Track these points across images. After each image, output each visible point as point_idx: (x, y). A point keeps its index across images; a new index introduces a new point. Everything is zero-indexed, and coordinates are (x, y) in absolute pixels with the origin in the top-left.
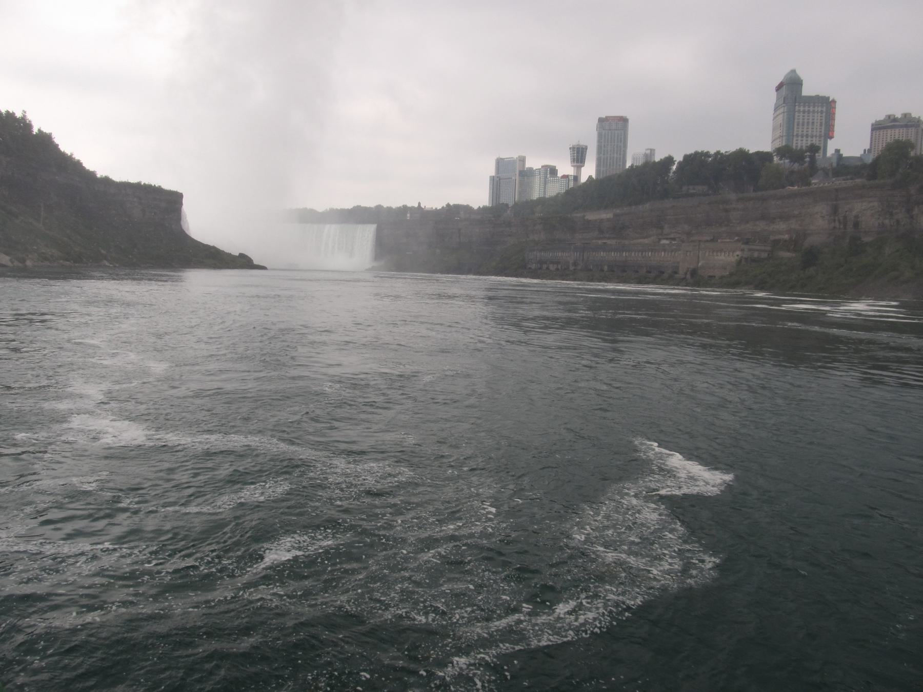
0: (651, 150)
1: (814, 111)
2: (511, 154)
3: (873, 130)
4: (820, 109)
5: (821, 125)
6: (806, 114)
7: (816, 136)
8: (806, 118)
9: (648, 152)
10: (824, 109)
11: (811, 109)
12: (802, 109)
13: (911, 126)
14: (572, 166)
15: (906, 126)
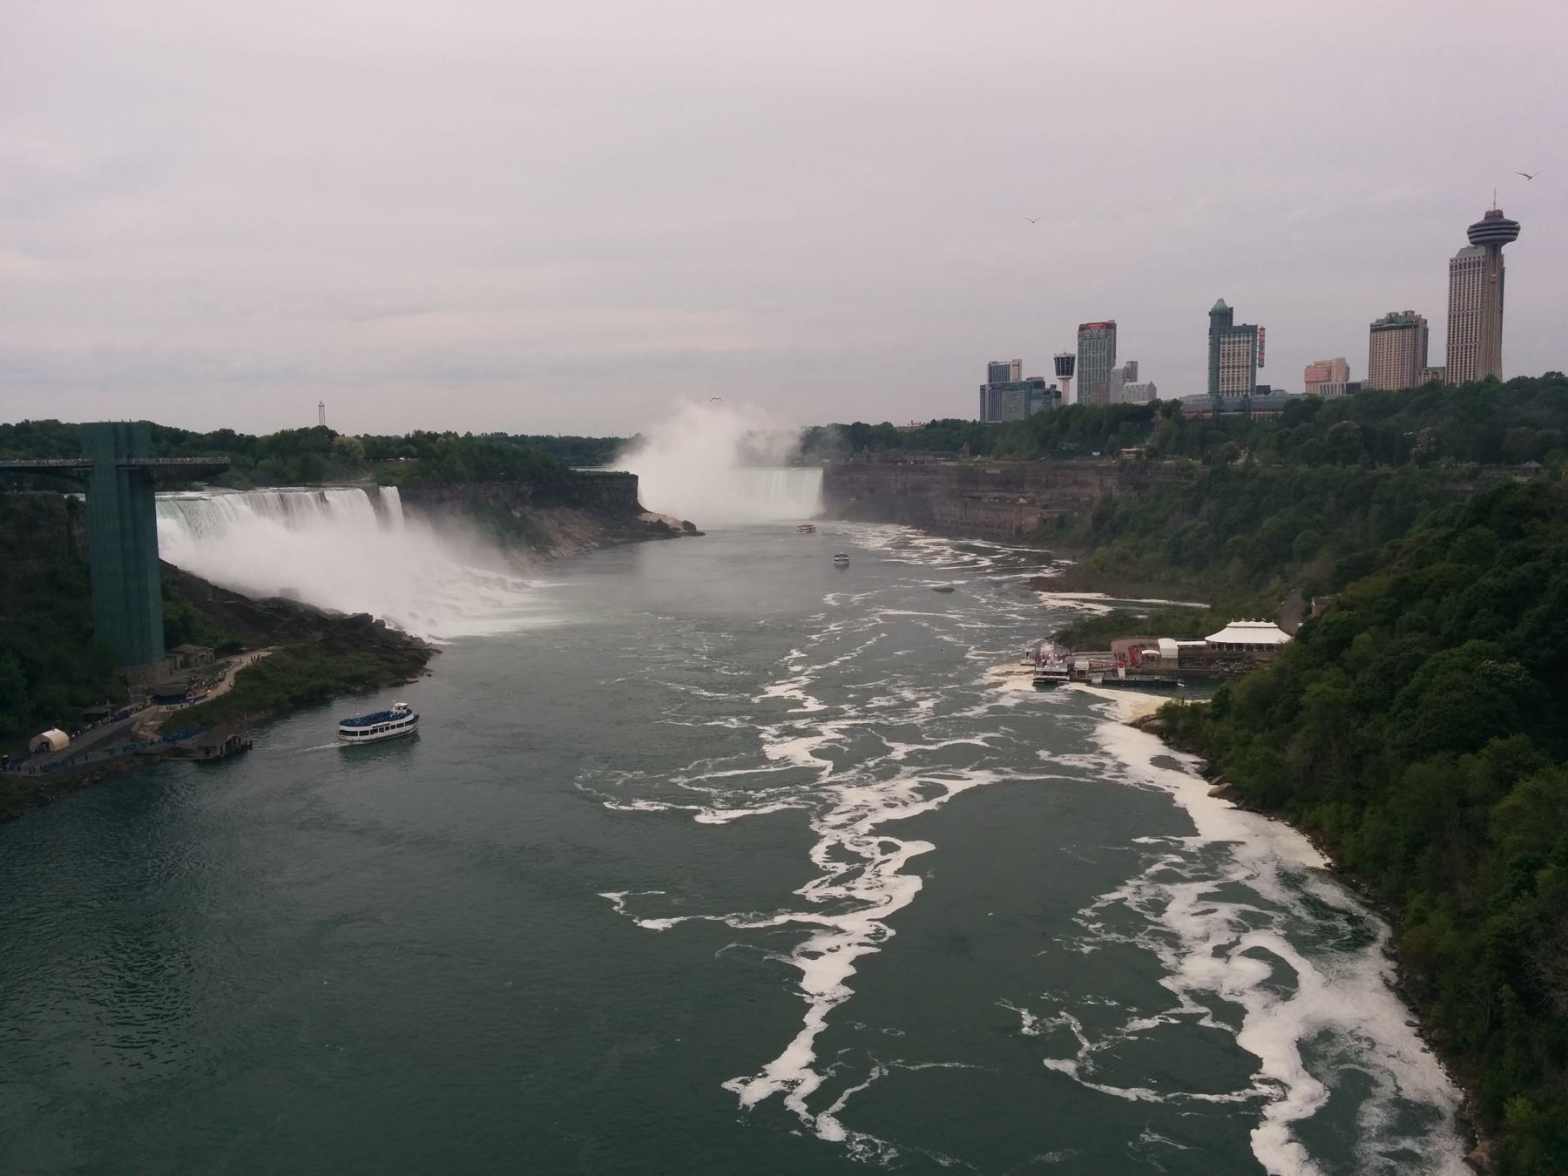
0: (1132, 362)
1: (1239, 342)
2: (1003, 358)
3: (1372, 331)
4: (1246, 339)
5: (1248, 355)
6: (1231, 345)
7: (1243, 367)
8: (1232, 349)
9: (1129, 366)
10: (1250, 338)
11: (1237, 339)
12: (1227, 339)
13: (1410, 327)
14: (1060, 379)
15: (1403, 328)
